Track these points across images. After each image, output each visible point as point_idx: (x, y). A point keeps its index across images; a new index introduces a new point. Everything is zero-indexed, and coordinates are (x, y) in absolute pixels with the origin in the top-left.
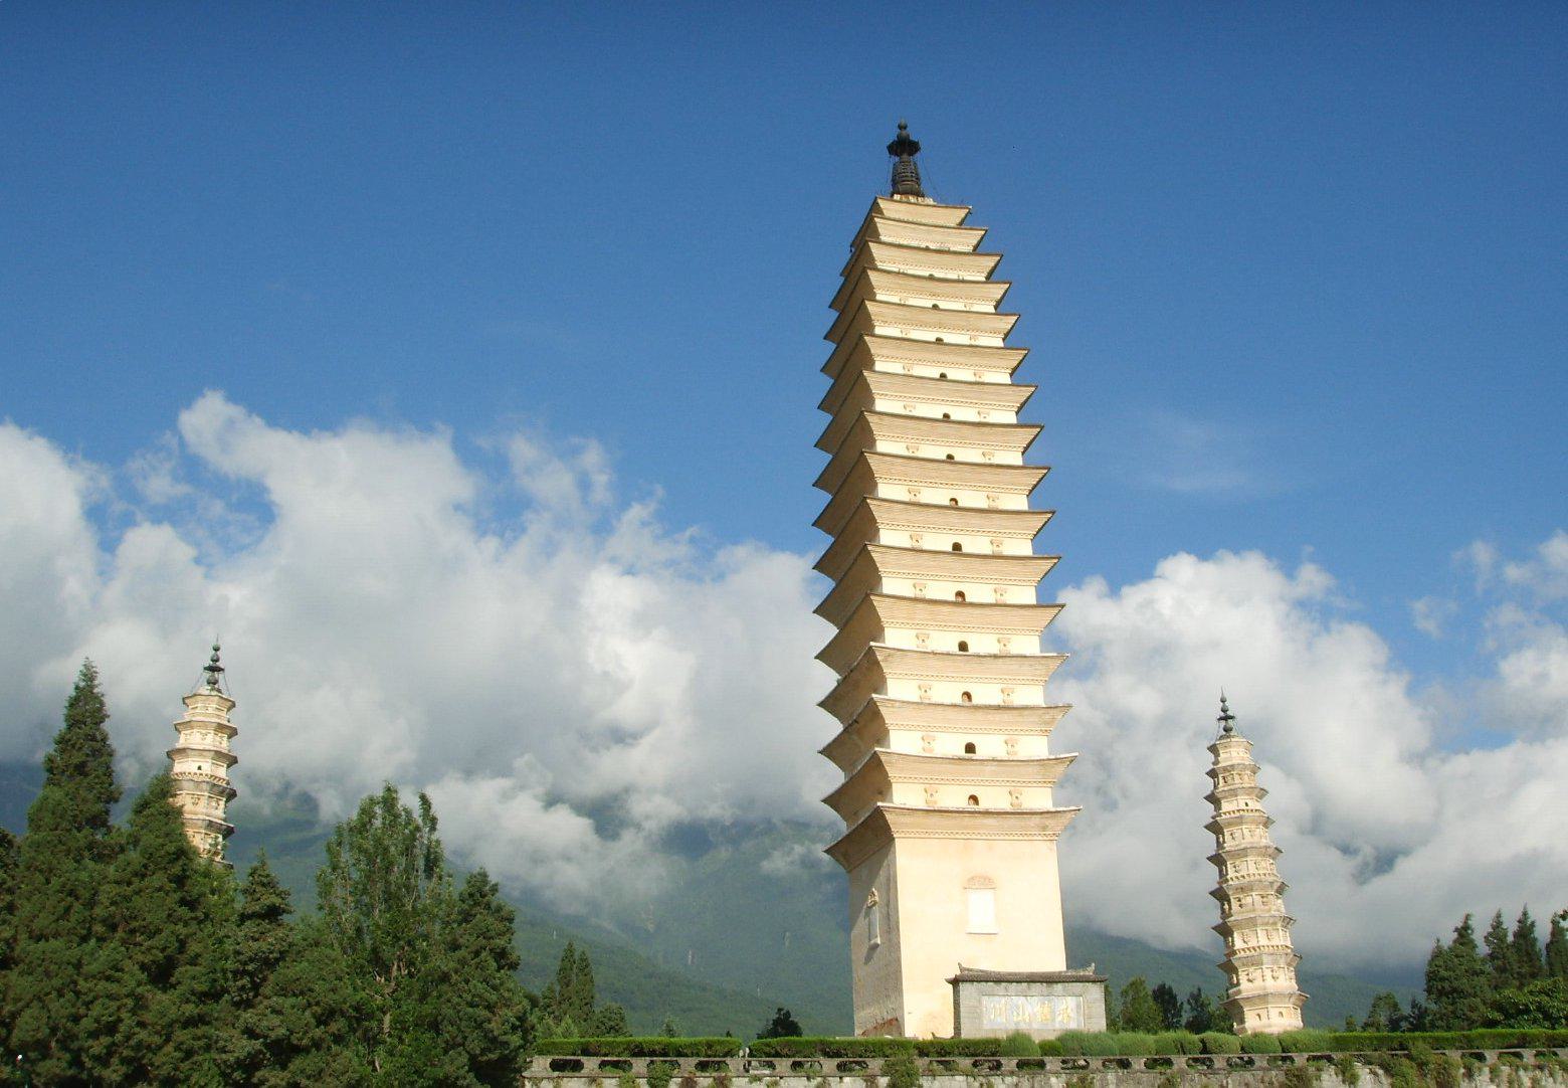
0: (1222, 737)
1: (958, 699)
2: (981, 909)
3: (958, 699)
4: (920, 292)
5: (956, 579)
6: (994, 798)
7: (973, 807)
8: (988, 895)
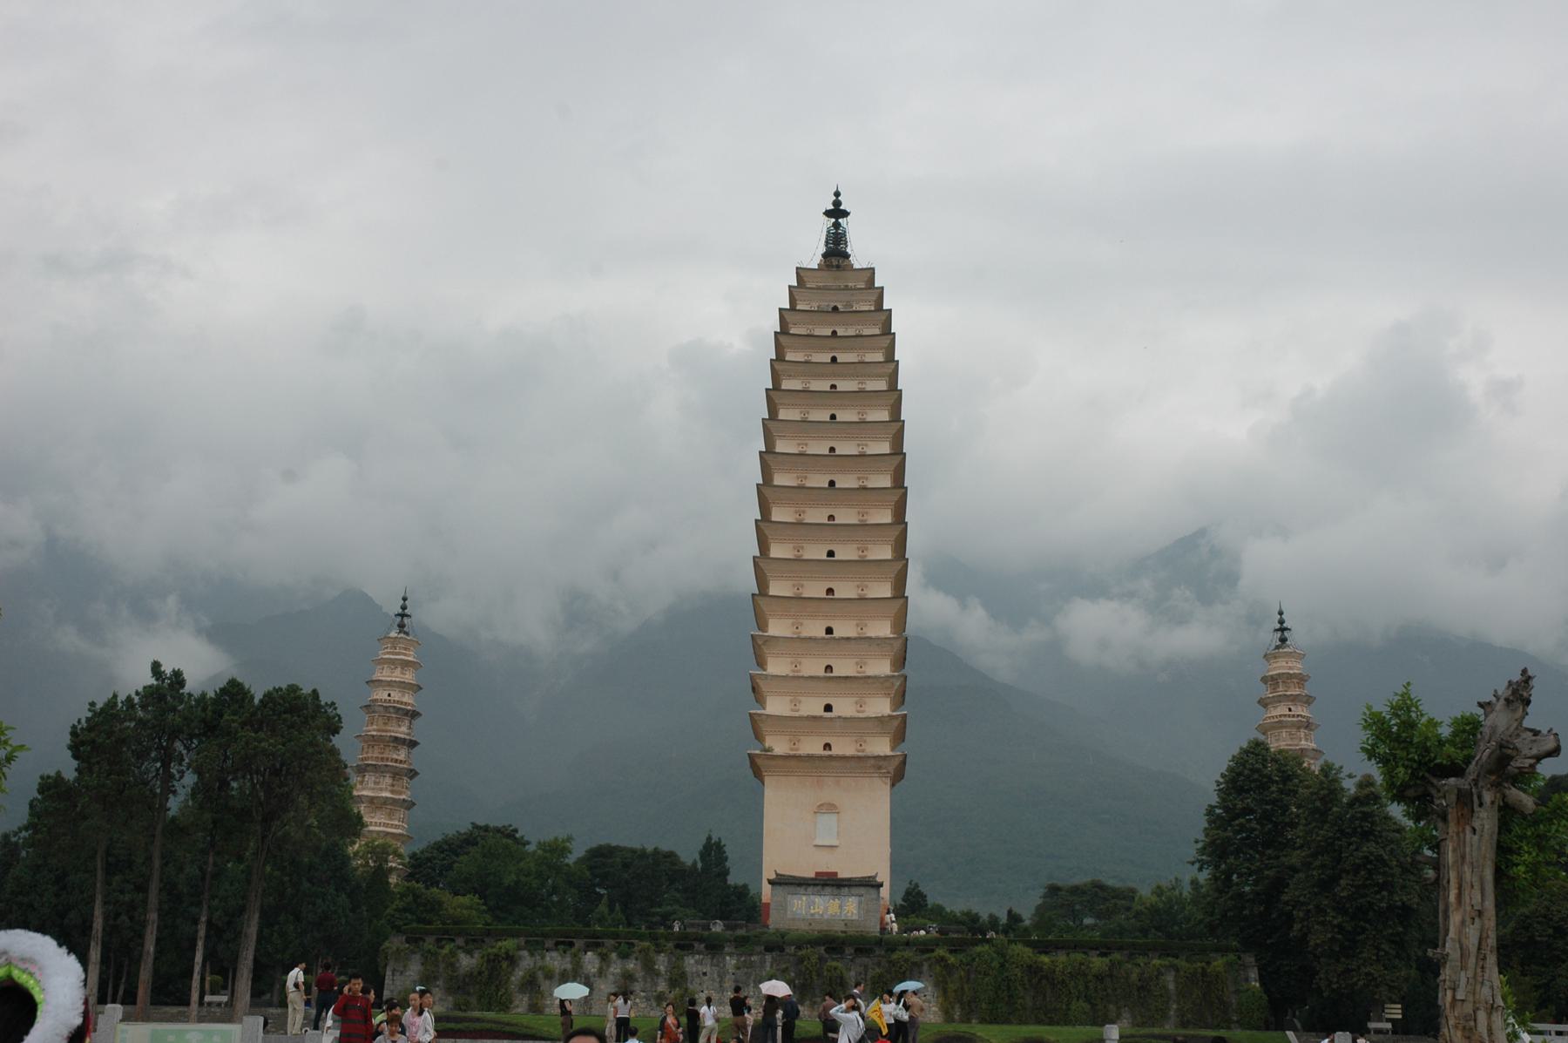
0: (1277, 647)
1: (821, 673)
2: (826, 830)
3: (821, 673)
4: (821, 349)
6: (844, 747)
7: (827, 753)
8: (834, 817)
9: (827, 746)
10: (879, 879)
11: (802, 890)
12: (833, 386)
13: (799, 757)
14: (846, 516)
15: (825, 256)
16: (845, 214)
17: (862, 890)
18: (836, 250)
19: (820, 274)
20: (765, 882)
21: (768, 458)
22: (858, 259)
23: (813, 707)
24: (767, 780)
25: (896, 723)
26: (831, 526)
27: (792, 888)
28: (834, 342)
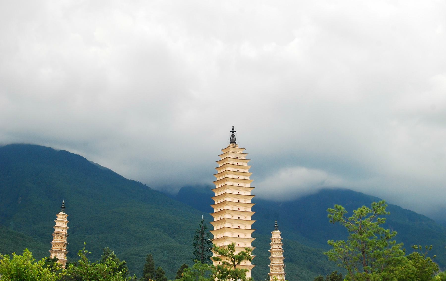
18: (233, 141)
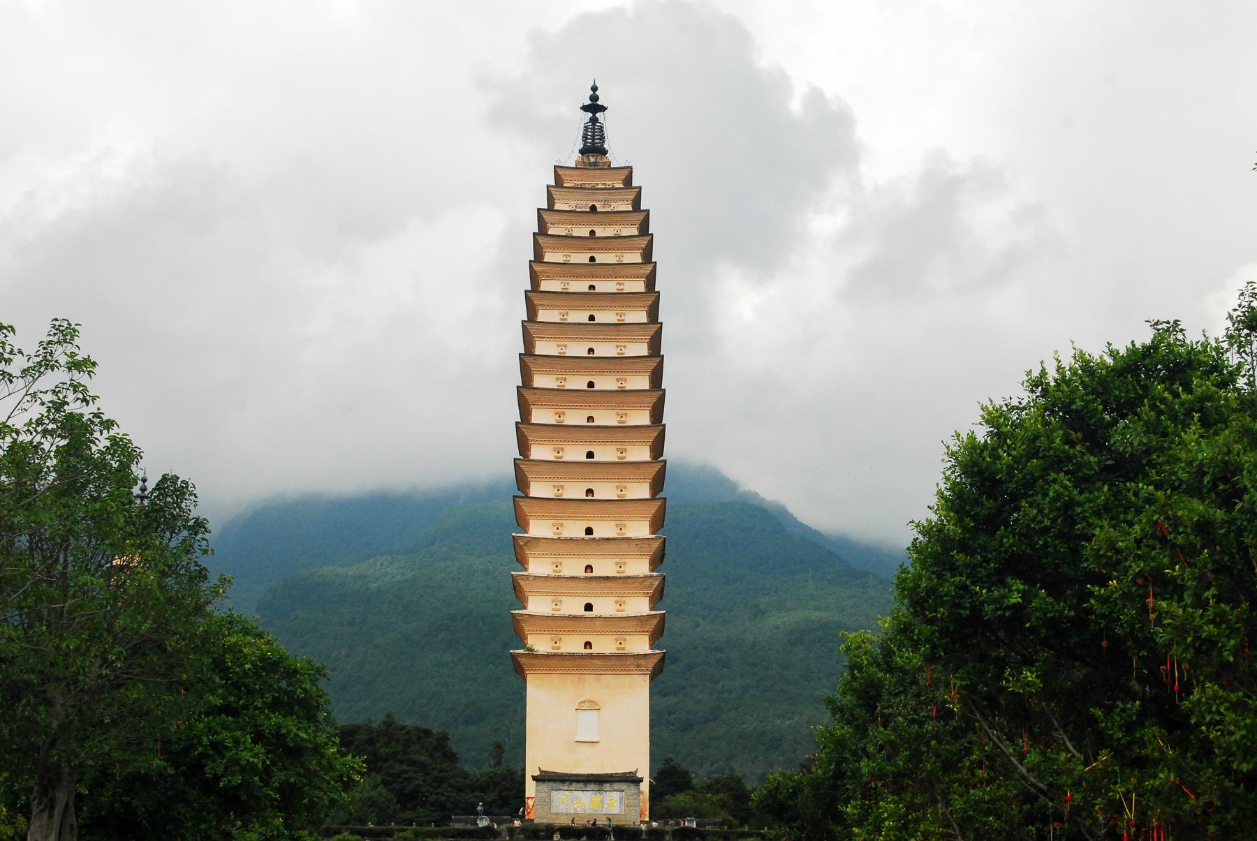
1: (581, 573)
2: (587, 725)
3: (581, 573)
4: (580, 249)
5: (586, 480)
6: (604, 645)
7: (588, 651)
9: (588, 645)
10: (639, 775)
11: (565, 787)
12: (592, 287)
13: (561, 656)
14: (605, 418)
15: (582, 152)
16: (603, 109)
17: (623, 786)
18: (594, 147)
19: (576, 172)
20: (529, 780)
21: (528, 361)
22: (616, 156)
23: (573, 606)
24: (529, 678)
25: (655, 622)
26: (592, 430)
27: (555, 785)
28: (590, 243)
